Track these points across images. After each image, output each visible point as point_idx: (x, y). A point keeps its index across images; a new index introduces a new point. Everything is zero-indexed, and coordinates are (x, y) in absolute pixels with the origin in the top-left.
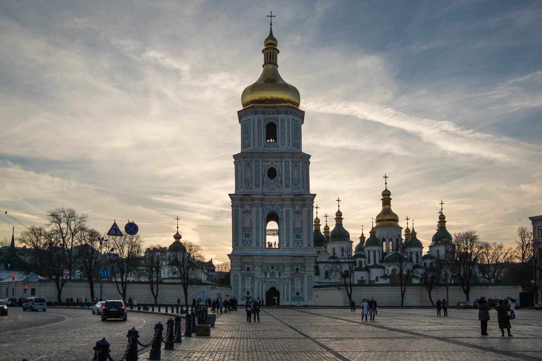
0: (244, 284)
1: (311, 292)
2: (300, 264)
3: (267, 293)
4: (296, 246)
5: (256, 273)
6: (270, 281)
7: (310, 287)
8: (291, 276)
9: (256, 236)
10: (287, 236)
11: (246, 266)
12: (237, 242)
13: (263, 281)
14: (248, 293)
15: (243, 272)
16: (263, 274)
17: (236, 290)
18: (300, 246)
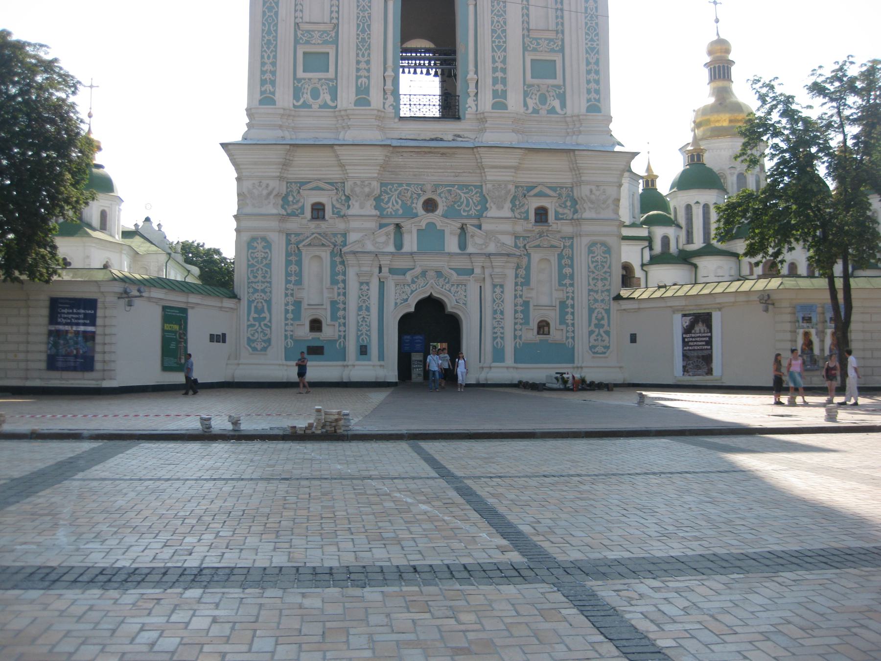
0: (299, 282)
1: (605, 322)
2: (553, 189)
3: (406, 323)
4: (536, 111)
5: (355, 230)
6: (418, 270)
7: (599, 297)
8: (516, 246)
9: (358, 62)
10: (494, 61)
11: (311, 198)
12: (268, 87)
13: (385, 270)
14: (316, 325)
15: (293, 225)
16: (387, 234)
17: (259, 311)
18: (552, 111)
